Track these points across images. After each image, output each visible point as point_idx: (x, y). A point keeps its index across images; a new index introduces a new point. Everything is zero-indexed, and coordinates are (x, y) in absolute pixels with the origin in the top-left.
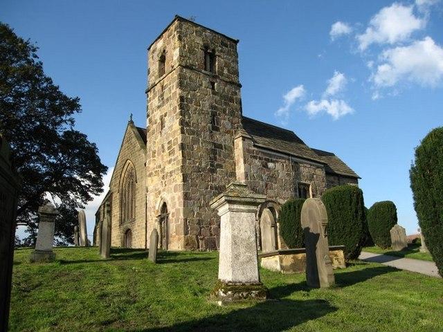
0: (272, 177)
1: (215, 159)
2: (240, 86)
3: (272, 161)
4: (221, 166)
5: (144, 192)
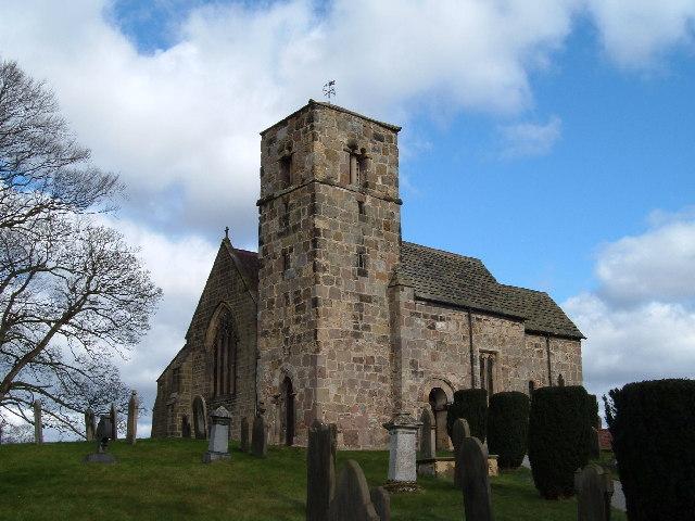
2: (399, 203)
3: (442, 319)
4: (367, 328)
5: (252, 358)
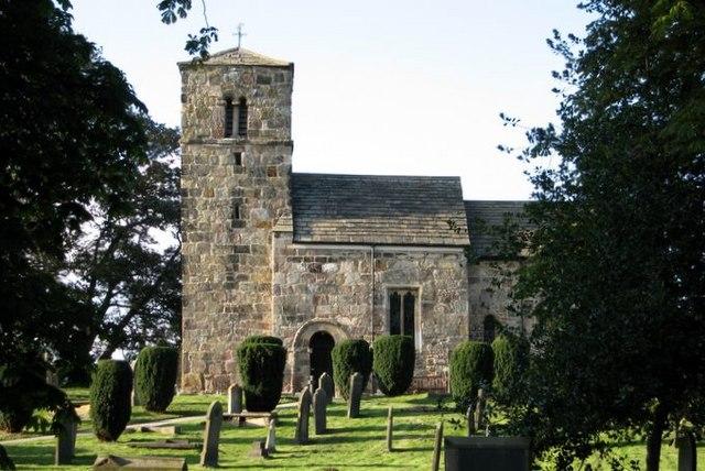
0: (329, 285)
1: (236, 268)
3: (331, 261)
4: (245, 278)
